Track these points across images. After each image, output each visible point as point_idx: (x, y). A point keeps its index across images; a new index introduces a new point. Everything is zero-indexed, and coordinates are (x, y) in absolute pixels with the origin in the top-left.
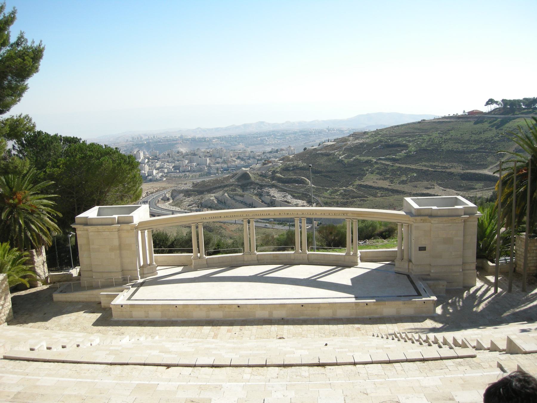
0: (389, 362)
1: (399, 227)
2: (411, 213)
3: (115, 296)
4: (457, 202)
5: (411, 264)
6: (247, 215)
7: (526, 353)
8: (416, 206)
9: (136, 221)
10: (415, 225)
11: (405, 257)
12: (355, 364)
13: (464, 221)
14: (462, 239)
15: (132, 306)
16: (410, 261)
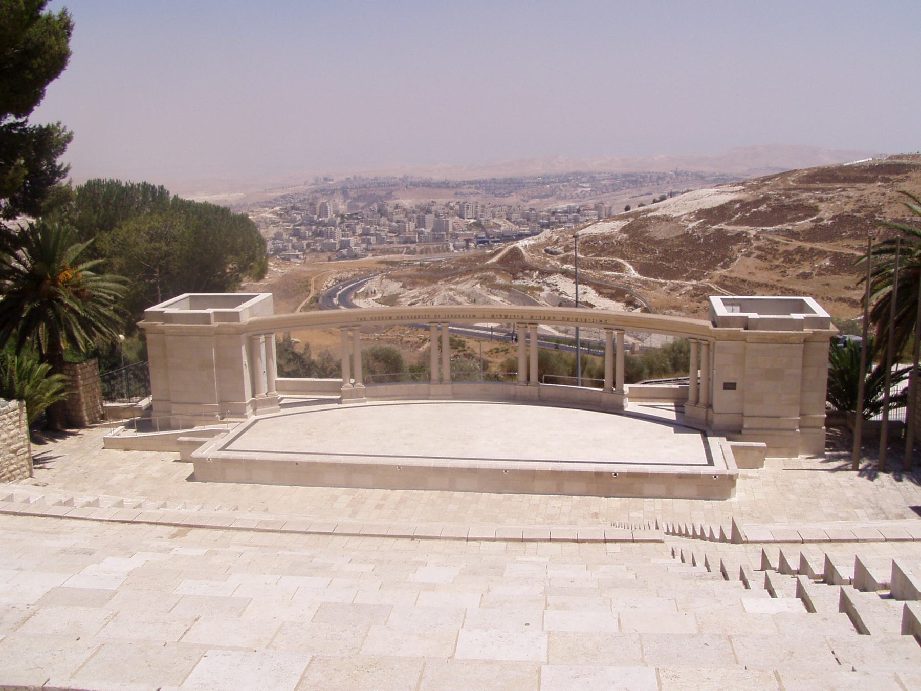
0: (523, 540)
1: (693, 348)
2: (717, 321)
3: (201, 443)
4: (802, 307)
5: (710, 411)
6: (436, 317)
7: (747, 542)
8: (721, 310)
9: (246, 319)
10: (718, 343)
11: (702, 399)
12: (468, 540)
13: (805, 341)
14: (799, 371)
15: (226, 461)
16: (709, 406)
